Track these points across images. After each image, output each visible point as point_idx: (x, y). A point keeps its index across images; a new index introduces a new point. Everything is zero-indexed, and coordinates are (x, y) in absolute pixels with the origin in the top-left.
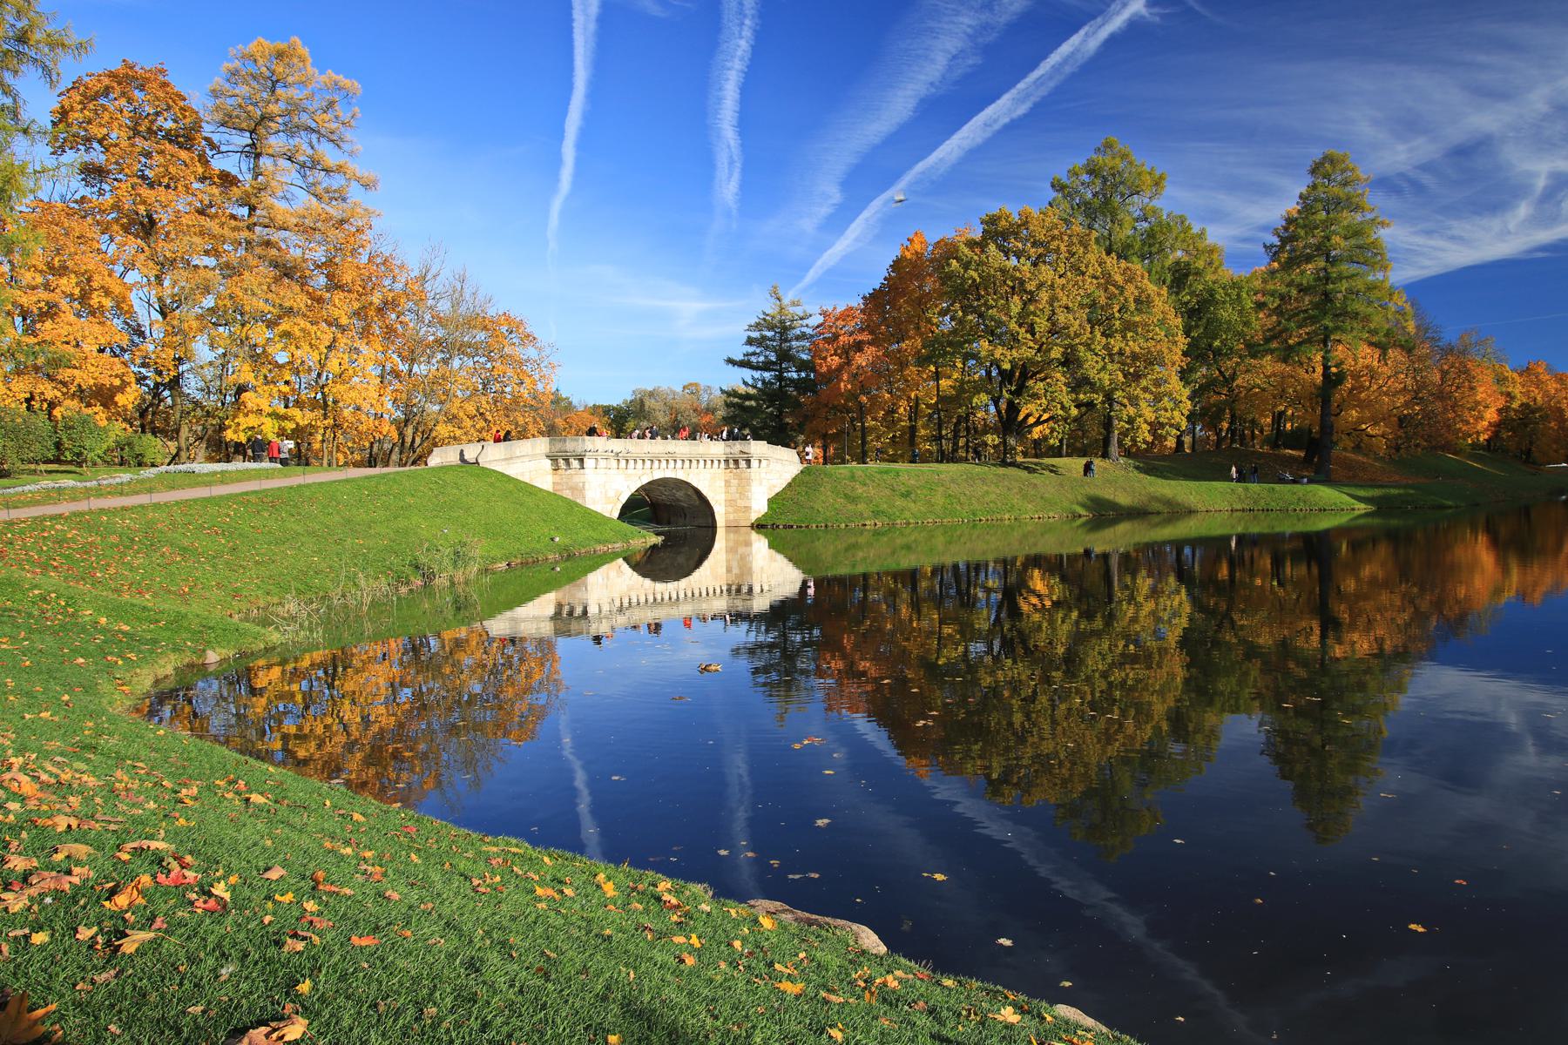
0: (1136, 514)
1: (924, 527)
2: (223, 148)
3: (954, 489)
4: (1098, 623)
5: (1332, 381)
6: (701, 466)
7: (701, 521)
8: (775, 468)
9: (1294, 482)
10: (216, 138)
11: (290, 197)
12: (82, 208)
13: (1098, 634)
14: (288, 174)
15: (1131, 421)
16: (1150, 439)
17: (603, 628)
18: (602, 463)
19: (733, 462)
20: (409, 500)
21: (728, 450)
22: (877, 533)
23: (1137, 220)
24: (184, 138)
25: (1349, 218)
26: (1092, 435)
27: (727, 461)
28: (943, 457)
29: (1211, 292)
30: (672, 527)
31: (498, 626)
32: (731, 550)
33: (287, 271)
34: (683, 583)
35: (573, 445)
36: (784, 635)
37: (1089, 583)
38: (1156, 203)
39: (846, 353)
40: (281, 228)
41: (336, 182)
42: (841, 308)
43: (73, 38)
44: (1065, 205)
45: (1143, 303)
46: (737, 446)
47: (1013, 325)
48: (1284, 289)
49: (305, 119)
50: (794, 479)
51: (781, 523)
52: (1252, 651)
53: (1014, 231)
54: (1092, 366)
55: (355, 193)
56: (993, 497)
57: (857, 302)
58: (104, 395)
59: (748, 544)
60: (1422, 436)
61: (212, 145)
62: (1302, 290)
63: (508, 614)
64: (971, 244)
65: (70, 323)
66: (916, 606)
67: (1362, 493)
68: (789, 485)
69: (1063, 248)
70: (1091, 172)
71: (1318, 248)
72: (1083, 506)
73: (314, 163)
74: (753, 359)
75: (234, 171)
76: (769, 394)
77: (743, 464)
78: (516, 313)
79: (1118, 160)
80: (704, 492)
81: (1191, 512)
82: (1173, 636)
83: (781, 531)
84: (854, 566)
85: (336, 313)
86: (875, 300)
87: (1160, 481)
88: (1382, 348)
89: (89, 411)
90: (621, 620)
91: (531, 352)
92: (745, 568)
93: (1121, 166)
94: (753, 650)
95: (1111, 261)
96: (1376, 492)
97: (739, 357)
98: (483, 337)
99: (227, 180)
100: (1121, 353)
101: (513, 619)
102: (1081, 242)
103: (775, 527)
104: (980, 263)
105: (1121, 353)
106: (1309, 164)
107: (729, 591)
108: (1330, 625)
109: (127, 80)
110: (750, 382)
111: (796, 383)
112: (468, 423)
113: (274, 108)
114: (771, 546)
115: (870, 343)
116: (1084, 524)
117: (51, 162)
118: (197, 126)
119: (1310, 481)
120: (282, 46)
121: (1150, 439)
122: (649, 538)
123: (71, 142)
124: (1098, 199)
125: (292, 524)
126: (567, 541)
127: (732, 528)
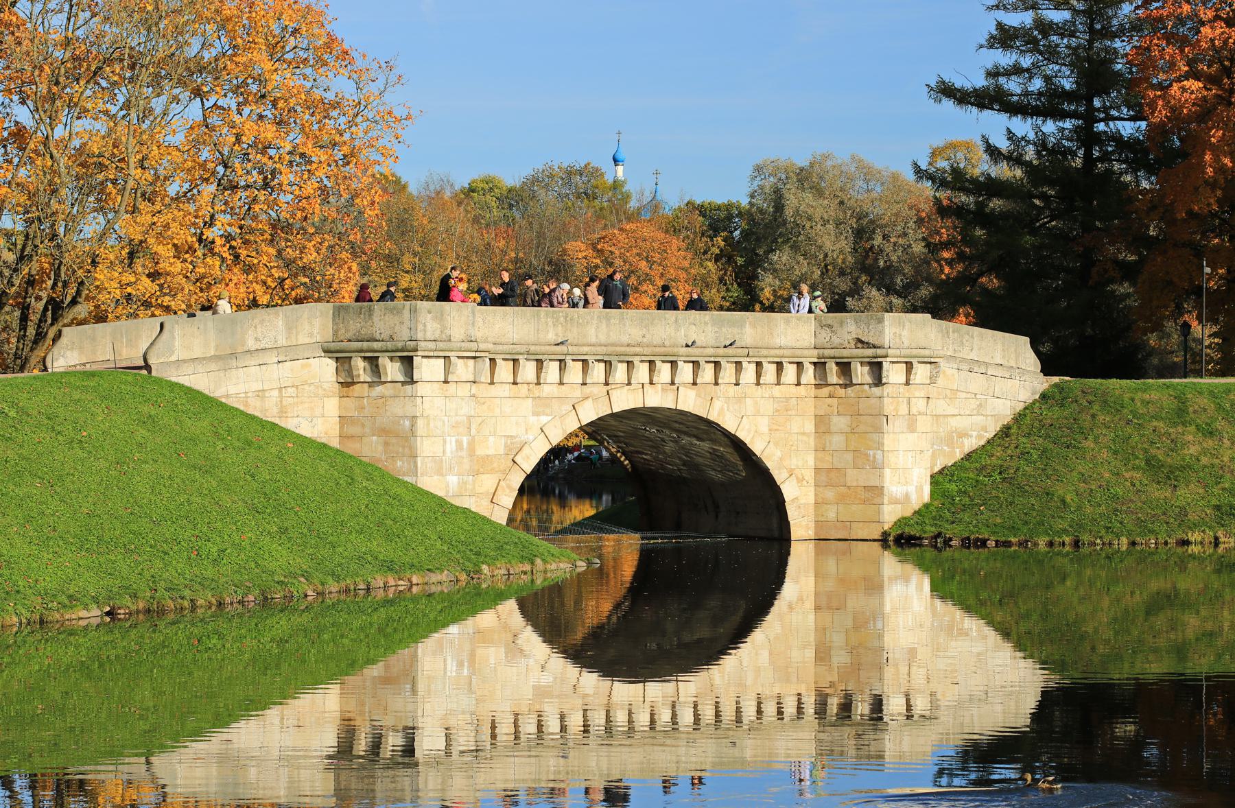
8: (963, 388)
19: (835, 369)
21: (825, 335)
27: (820, 366)
30: (670, 540)
32: (826, 604)
34: (690, 686)
35: (384, 322)
46: (849, 327)
50: (1019, 418)
51: (955, 532)
59: (874, 586)
63: (214, 743)
68: (1005, 431)
74: (1013, 85)
77: (861, 373)
80: (757, 447)
83: (955, 552)
84: (1180, 651)
92: (866, 651)
101: (230, 760)
103: (940, 542)
107: (821, 711)
110: (1003, 144)
114: (940, 590)
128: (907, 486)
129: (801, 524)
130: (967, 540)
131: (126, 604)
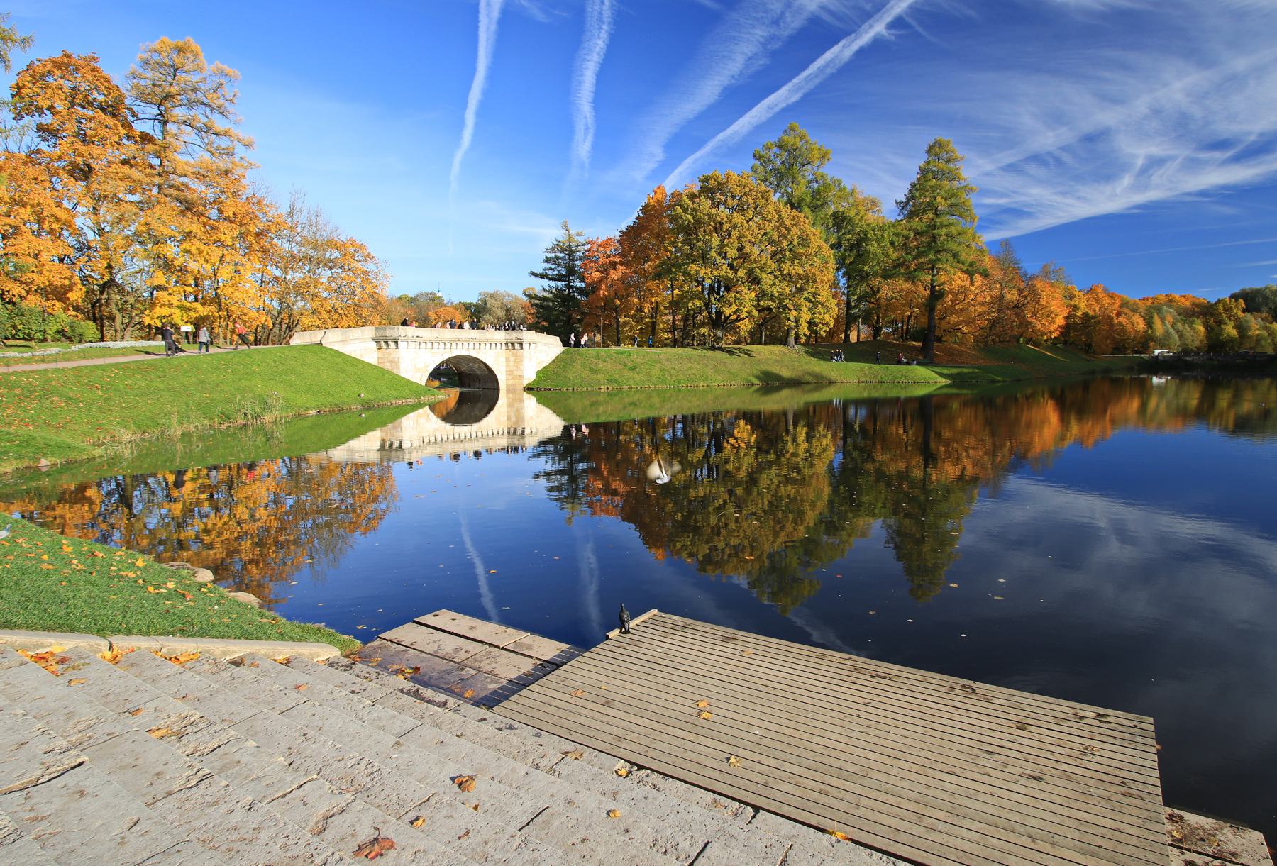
0: (795, 383)
1: (642, 391)
2: (140, 116)
3: (668, 365)
4: (772, 457)
5: (936, 295)
6: (488, 348)
7: (489, 385)
8: (544, 349)
9: (907, 363)
10: (135, 108)
11: (189, 153)
12: (33, 157)
13: (770, 464)
14: (190, 135)
15: (796, 321)
16: (808, 333)
17: (414, 457)
20: (255, 368)
22: (609, 394)
23: (810, 182)
24: (112, 109)
25: (947, 184)
26: (771, 328)
28: (675, 343)
29: (865, 233)
30: (469, 389)
31: (339, 454)
32: (510, 405)
33: (188, 207)
35: (390, 332)
36: (571, 464)
37: (770, 430)
39: (605, 270)
40: (181, 176)
41: (223, 142)
42: (603, 238)
43: (19, 34)
44: (760, 169)
45: (804, 241)
46: (514, 334)
47: (713, 253)
48: (905, 232)
49: (200, 95)
52: (880, 476)
53: (721, 186)
54: (767, 279)
55: (240, 150)
56: (694, 371)
57: (617, 235)
58: (59, 293)
59: (522, 401)
60: (1006, 336)
61: (134, 114)
62: (918, 233)
63: (343, 447)
64: (692, 197)
65: (25, 242)
67: (946, 371)
69: (751, 201)
70: (780, 147)
71: (929, 204)
72: (757, 377)
73: (208, 129)
74: (549, 273)
75: (151, 133)
76: (564, 298)
77: (517, 346)
78: (358, 239)
79: (797, 139)
81: (831, 383)
82: (821, 468)
83: (543, 391)
84: (598, 416)
85: (223, 237)
86: (631, 234)
87: (822, 362)
88: (971, 275)
89: (49, 303)
90: (431, 450)
92: (520, 418)
93: (799, 144)
94: (548, 474)
95: (786, 211)
96: (955, 371)
98: (338, 256)
99: (146, 138)
100: (789, 274)
101: (350, 450)
102: (763, 197)
103: (539, 389)
104: (695, 210)
105: (789, 274)
106: (925, 147)
108: (929, 458)
109: (65, 66)
111: (580, 290)
112: (325, 316)
113: (174, 90)
115: (621, 263)
116: (758, 390)
117: (11, 123)
118: (120, 100)
119: (918, 363)
120: (181, 43)
121: (808, 333)
122: (451, 395)
123: (34, 108)
124: (784, 165)
125: (157, 384)
126: (371, 397)
128: (529, 376)
129: (503, 385)
130: (544, 389)
131: (323, 410)
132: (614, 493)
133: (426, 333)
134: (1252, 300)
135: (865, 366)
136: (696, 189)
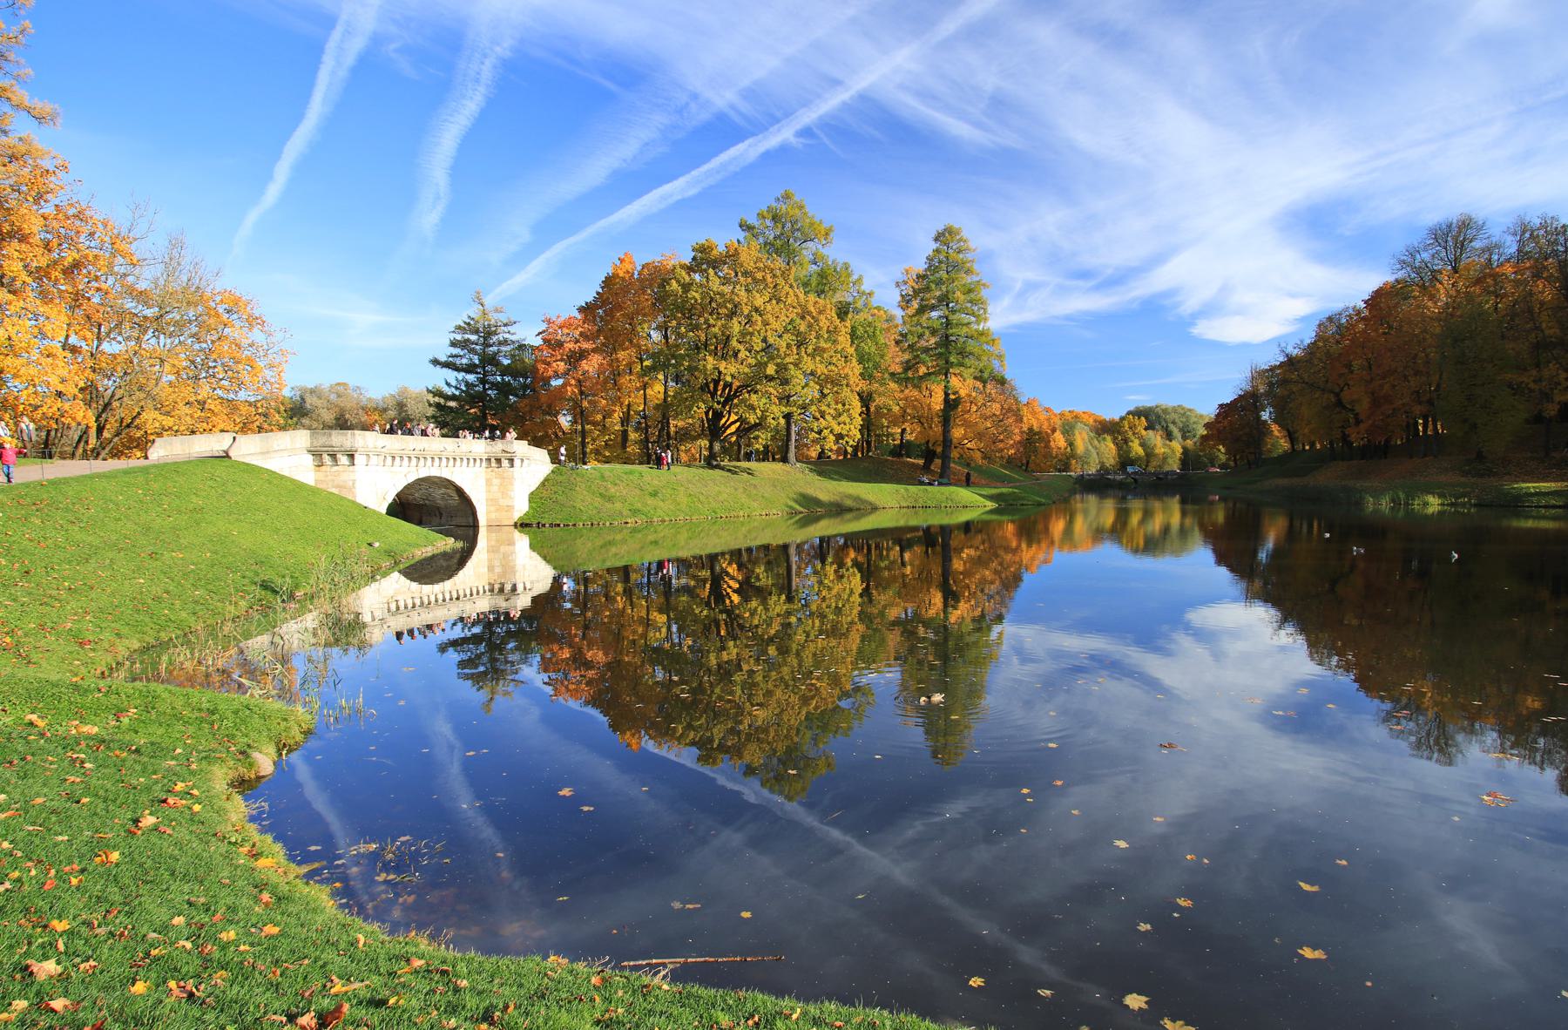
18: (374, 459)
21: (489, 449)
32: (492, 550)
38: (824, 251)
39: (576, 358)
46: (499, 446)
59: (511, 543)
66: (628, 593)
68: (543, 484)
74: (458, 361)
76: (470, 397)
77: (505, 463)
81: (875, 509)
83: (547, 529)
91: (257, 335)
92: (508, 568)
97: (443, 359)
98: (192, 315)
107: (492, 590)
108: (951, 597)
110: (454, 383)
127: (494, 527)
129: (482, 520)
132: (588, 665)
133: (398, 442)
134: (1151, 417)
135: (902, 488)
136: (687, 260)
